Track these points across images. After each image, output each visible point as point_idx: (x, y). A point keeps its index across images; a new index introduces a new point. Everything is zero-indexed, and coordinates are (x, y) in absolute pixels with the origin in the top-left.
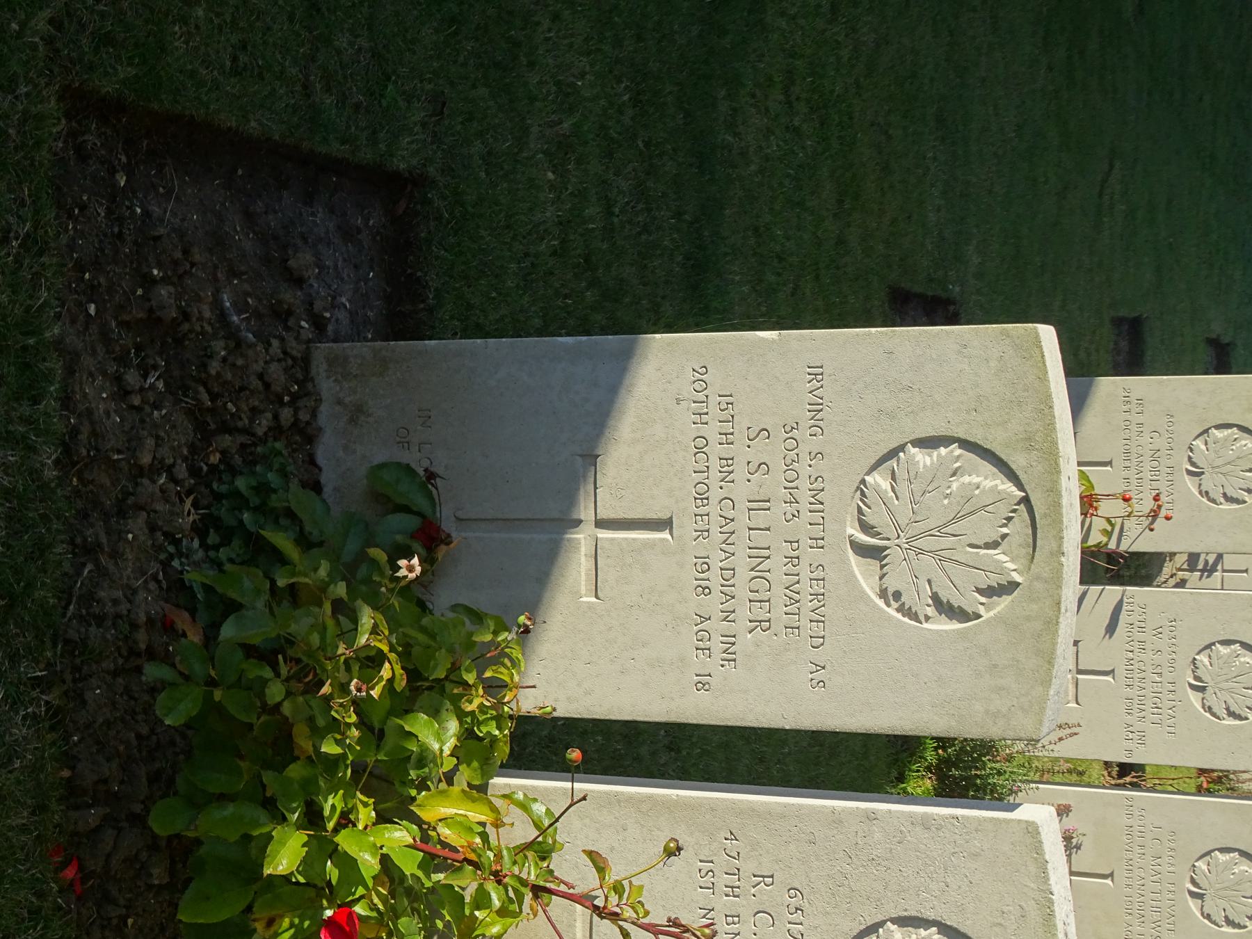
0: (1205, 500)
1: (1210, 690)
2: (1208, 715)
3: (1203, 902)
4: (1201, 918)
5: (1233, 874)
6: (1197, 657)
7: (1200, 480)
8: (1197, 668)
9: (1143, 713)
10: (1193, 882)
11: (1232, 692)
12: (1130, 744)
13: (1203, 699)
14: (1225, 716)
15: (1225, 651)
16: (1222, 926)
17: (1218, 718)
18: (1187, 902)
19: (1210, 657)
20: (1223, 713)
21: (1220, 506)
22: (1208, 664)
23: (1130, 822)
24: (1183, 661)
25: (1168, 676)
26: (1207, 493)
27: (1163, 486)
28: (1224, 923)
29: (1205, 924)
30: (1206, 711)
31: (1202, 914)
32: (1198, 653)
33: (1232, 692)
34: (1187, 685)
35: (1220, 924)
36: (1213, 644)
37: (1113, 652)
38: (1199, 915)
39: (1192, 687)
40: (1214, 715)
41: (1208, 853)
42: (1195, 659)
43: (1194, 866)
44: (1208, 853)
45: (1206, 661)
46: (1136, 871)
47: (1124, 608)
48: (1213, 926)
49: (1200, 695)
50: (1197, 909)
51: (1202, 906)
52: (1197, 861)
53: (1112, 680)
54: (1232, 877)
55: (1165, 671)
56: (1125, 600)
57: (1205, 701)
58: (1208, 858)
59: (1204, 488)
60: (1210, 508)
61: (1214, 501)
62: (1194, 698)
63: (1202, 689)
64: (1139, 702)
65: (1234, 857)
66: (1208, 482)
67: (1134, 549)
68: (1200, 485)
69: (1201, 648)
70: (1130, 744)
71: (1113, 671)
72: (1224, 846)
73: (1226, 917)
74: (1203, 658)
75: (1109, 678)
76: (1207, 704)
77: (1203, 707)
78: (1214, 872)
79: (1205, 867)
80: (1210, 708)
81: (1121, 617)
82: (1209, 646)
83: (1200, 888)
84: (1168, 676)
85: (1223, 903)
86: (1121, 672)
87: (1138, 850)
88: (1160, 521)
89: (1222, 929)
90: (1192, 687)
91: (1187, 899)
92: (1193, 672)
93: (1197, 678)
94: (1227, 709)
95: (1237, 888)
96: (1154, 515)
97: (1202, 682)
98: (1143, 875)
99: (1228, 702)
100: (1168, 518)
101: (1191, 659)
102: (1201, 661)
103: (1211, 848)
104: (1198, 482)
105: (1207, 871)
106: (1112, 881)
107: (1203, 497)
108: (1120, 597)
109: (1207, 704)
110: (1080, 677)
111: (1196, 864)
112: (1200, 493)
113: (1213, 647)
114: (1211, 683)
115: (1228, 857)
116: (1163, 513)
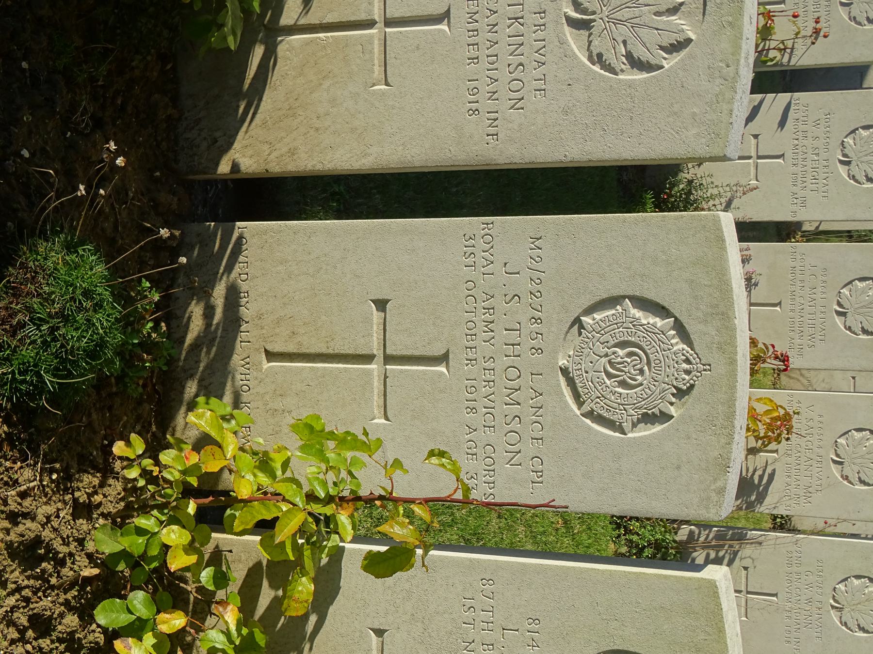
0: (853, 23)
1: (854, 163)
2: (852, 181)
3: (846, 318)
4: (845, 330)
5: (868, 296)
6: (845, 140)
7: (850, 9)
8: (845, 148)
9: (805, 184)
10: (839, 304)
11: (870, 163)
12: (794, 208)
13: (849, 170)
14: (865, 182)
15: (866, 134)
16: (859, 335)
17: (860, 183)
18: (835, 319)
19: (854, 139)
20: (864, 179)
21: (864, 27)
22: (853, 144)
23: (793, 264)
24: (835, 143)
25: (823, 155)
26: (855, 18)
27: (822, 14)
28: (860, 332)
29: (846, 333)
30: (850, 179)
31: (845, 327)
32: (846, 137)
33: (870, 163)
34: (837, 161)
35: (858, 333)
36: (857, 129)
37: (784, 141)
38: (843, 328)
39: (841, 162)
40: (857, 181)
41: (850, 282)
42: (843, 141)
43: (840, 292)
44: (850, 282)
45: (851, 142)
46: (798, 299)
47: (792, 108)
48: (853, 335)
49: (847, 167)
50: (841, 324)
51: (845, 321)
52: (842, 289)
53: (782, 162)
54: (867, 298)
55: (821, 152)
56: (793, 102)
57: (850, 171)
58: (850, 286)
59: (852, 15)
60: (856, 29)
61: (860, 24)
62: (842, 170)
63: (848, 163)
64: (802, 176)
65: (869, 285)
66: (855, 11)
67: (800, 63)
68: (850, 12)
69: (848, 133)
70: (794, 208)
71: (783, 155)
72: (862, 276)
73: (863, 328)
74: (849, 140)
75: (780, 161)
76: (852, 174)
77: (849, 176)
78: (854, 296)
79: (847, 293)
80: (854, 176)
81: (789, 114)
82: (853, 131)
83: (844, 308)
84: (823, 155)
85: (860, 318)
86: (789, 155)
87: (799, 283)
88: (821, 39)
89: (860, 337)
90: (841, 162)
91: (834, 316)
92: (842, 151)
93: (845, 155)
94: (866, 176)
95: (869, 306)
96: (817, 32)
97: (848, 157)
98: (802, 302)
99: (867, 171)
100: (825, 36)
101: (840, 142)
102: (848, 142)
103: (853, 279)
104: (849, 10)
105: (849, 295)
106: (780, 308)
107: (851, 21)
108: (789, 100)
109: (852, 174)
110: (759, 161)
111: (841, 291)
112: (850, 19)
113: (857, 132)
114: (855, 158)
115: (864, 284)
116: (822, 34)
